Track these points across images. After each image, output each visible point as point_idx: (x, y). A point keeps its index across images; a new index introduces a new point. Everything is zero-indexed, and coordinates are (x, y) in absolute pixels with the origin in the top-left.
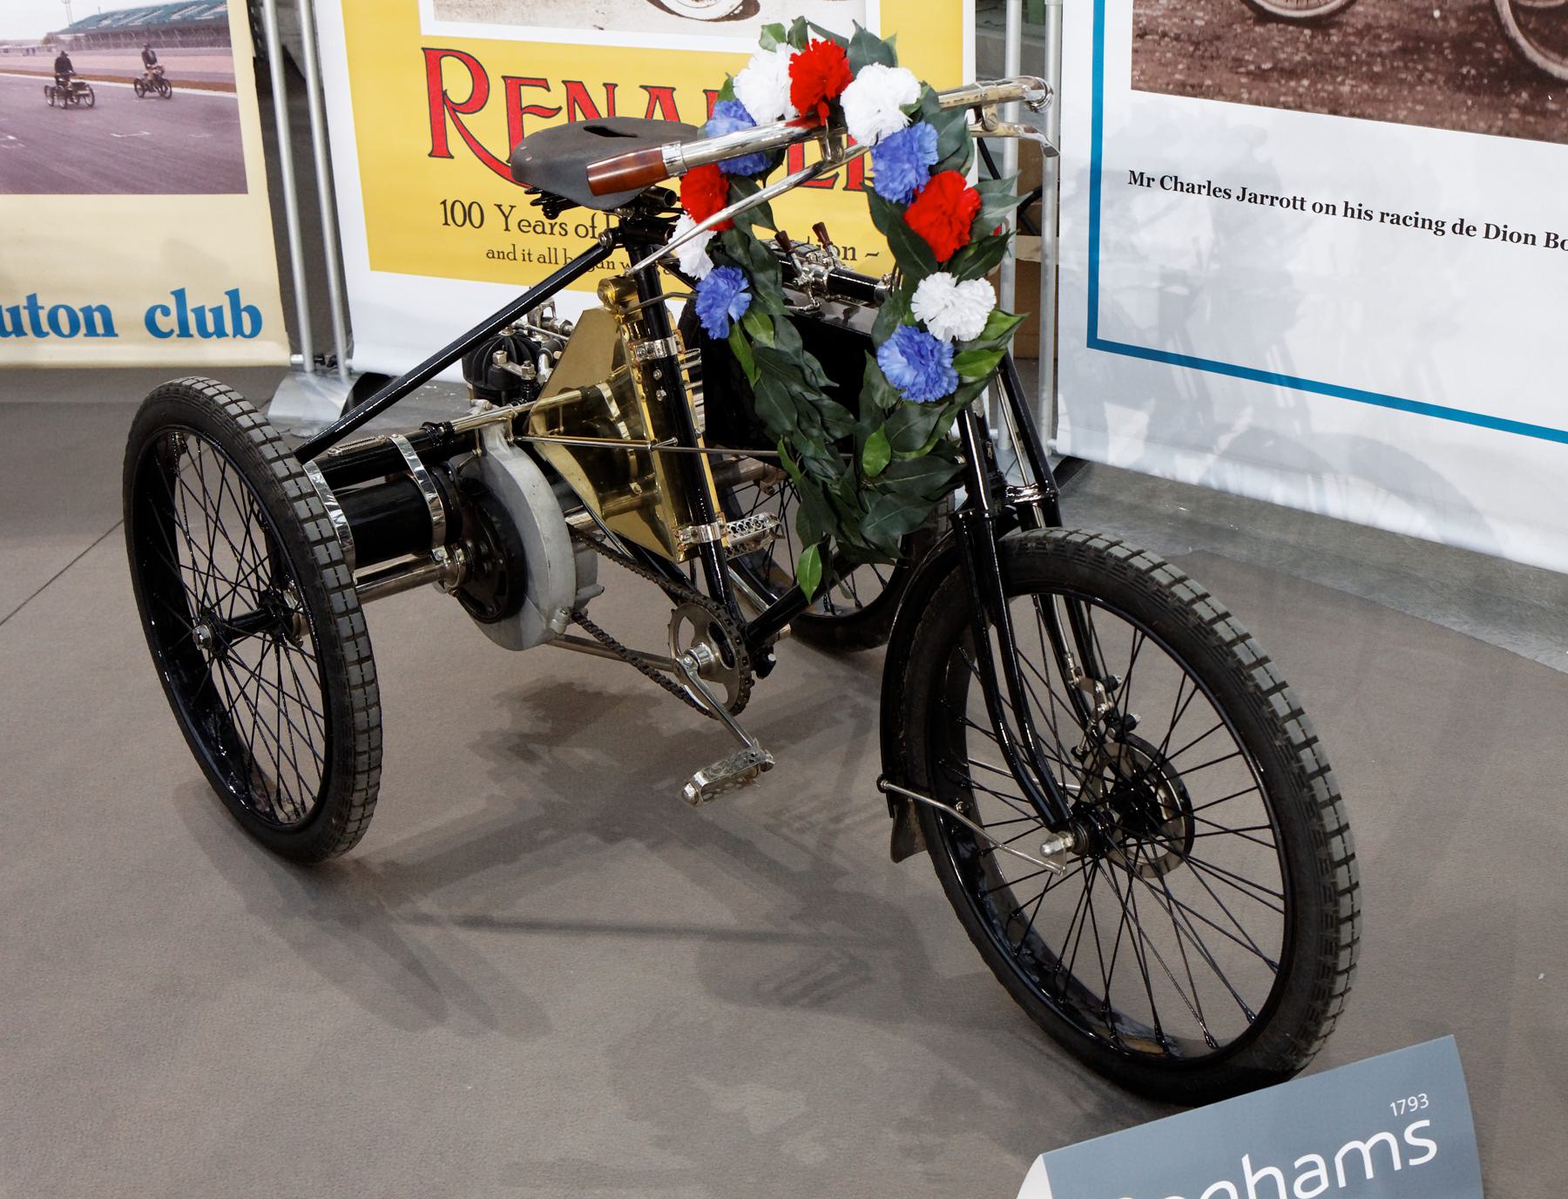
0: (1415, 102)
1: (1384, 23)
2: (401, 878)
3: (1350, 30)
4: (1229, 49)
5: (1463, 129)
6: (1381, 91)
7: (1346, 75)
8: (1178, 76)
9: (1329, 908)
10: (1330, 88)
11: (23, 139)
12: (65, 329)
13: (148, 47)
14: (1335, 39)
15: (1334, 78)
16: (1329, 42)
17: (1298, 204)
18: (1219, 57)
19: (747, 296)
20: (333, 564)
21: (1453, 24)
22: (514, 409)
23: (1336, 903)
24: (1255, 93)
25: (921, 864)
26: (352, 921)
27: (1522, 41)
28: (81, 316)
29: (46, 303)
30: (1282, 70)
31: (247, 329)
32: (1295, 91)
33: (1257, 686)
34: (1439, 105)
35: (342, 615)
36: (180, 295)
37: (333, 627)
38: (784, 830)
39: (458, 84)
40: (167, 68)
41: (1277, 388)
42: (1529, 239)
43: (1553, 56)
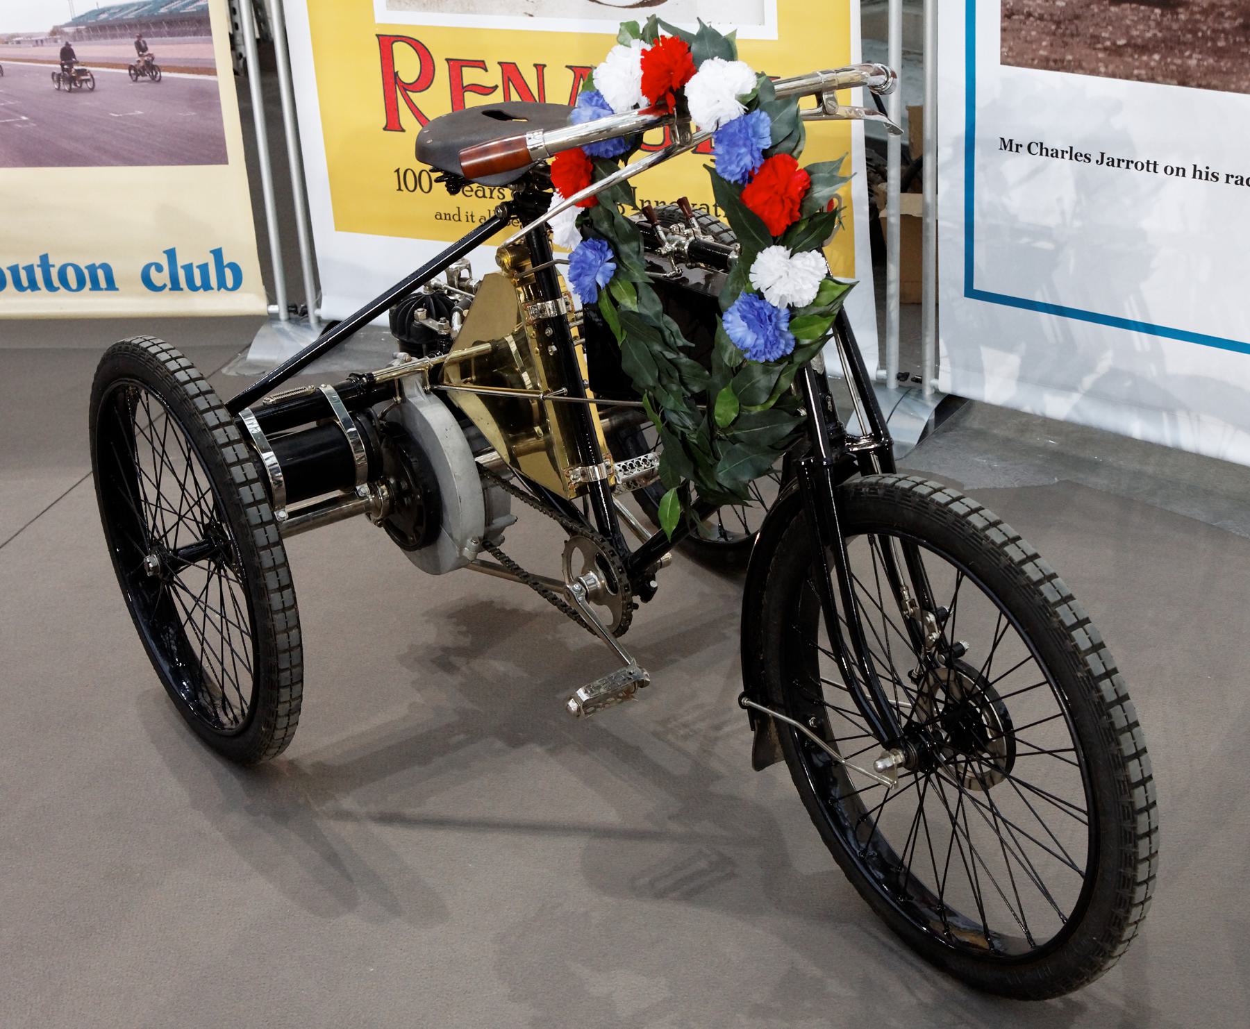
2: (329, 778)
3: (1196, 9)
6: (1225, 64)
7: (1193, 50)
8: (1042, 53)
9: (1127, 825)
10: (1179, 62)
11: (34, 119)
12: (74, 285)
13: (140, 37)
14: (1182, 17)
15: (1182, 52)
16: (1177, 20)
17: (1151, 167)
18: (1078, 35)
19: (612, 266)
20: (256, 503)
22: (429, 361)
23: (1134, 821)
24: (1111, 67)
25: (780, 771)
26: (281, 816)
28: (86, 272)
29: (56, 261)
31: (230, 282)
32: (1147, 65)
33: (1061, 622)
35: (264, 548)
36: (171, 254)
37: (256, 559)
38: (670, 737)
39: (407, 65)
40: (157, 56)
41: (1134, 333)
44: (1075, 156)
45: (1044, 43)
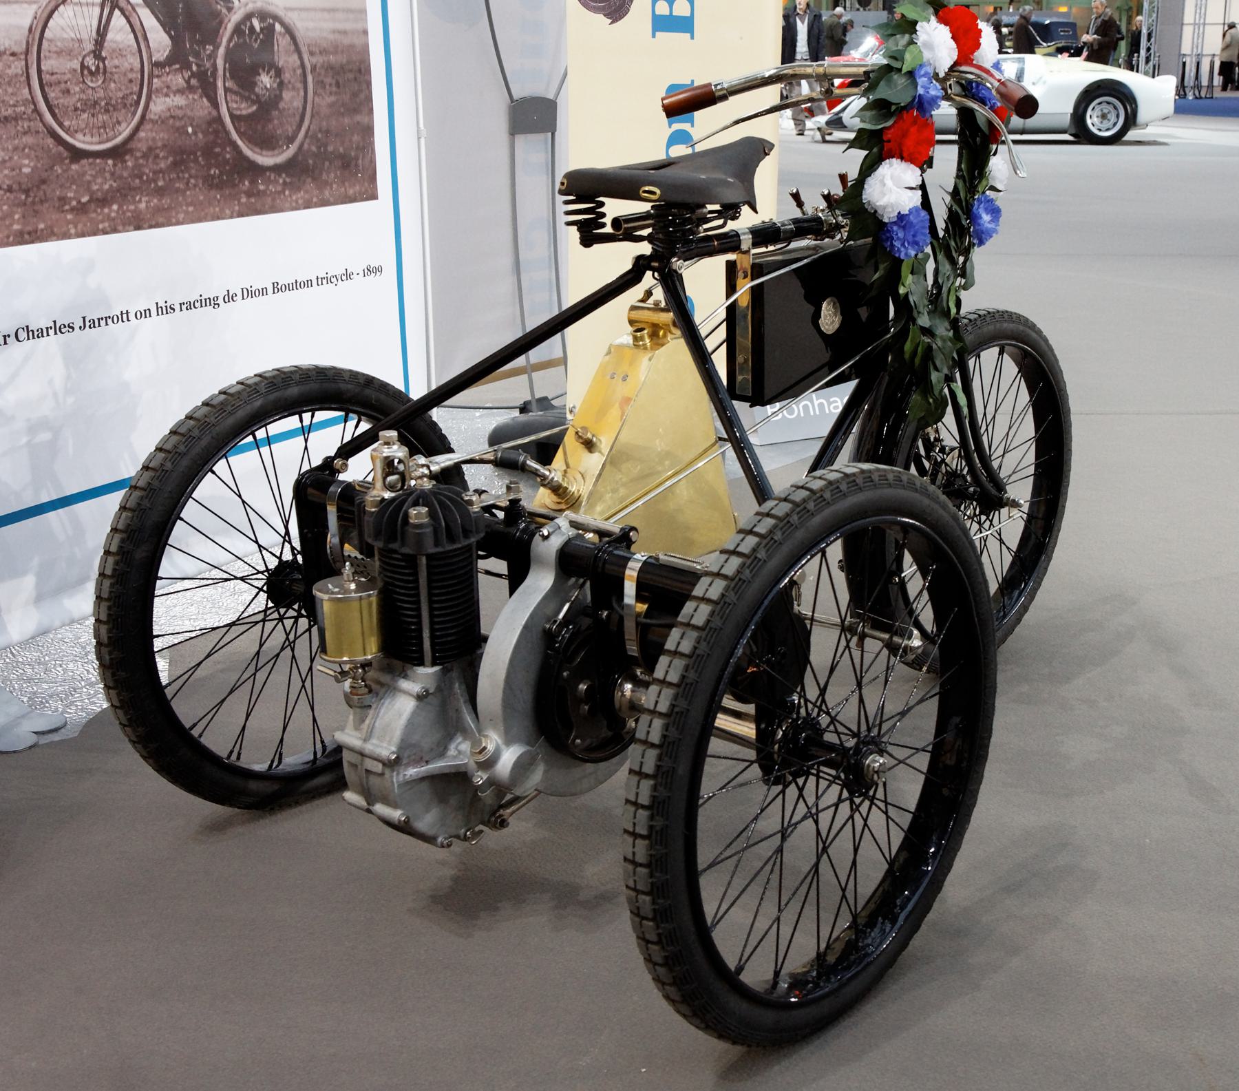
0: (188, 205)
1: (160, 144)
3: (138, 154)
4: (54, 191)
5: (218, 218)
6: (166, 201)
8: (16, 227)
10: (132, 207)
14: (129, 164)
15: (134, 197)
18: (46, 200)
21: (200, 135)
24: (80, 226)
27: (239, 142)
30: (97, 199)
32: (109, 218)
34: (201, 203)
42: (263, 292)
43: (257, 150)
44: (58, 329)
45: (17, 217)
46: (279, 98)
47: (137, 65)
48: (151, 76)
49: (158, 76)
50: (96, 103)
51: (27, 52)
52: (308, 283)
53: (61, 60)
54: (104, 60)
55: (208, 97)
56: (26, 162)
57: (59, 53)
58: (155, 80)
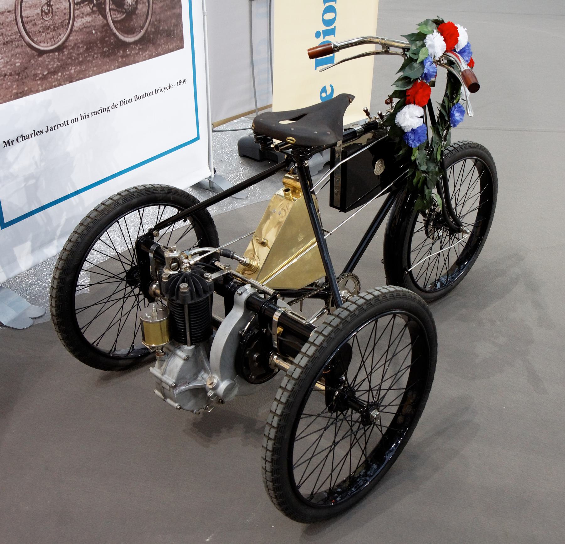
1: (80, 41)
5: (108, 71)
6: (83, 67)
7: (72, 66)
8: (14, 91)
10: (68, 73)
14: (66, 53)
15: (68, 68)
21: (99, 34)
24: (44, 86)
27: (117, 33)
32: (57, 79)
41: (72, 198)
42: (130, 101)
43: (126, 35)
44: (36, 134)
45: (14, 87)
46: (136, 8)
47: (68, 6)
48: (74, 10)
49: (78, 9)
50: (49, 27)
51: (15, 9)
52: (151, 94)
53: (32, 10)
54: (52, 6)
55: (102, 16)
56: (18, 61)
57: (30, 7)
58: (76, 11)
